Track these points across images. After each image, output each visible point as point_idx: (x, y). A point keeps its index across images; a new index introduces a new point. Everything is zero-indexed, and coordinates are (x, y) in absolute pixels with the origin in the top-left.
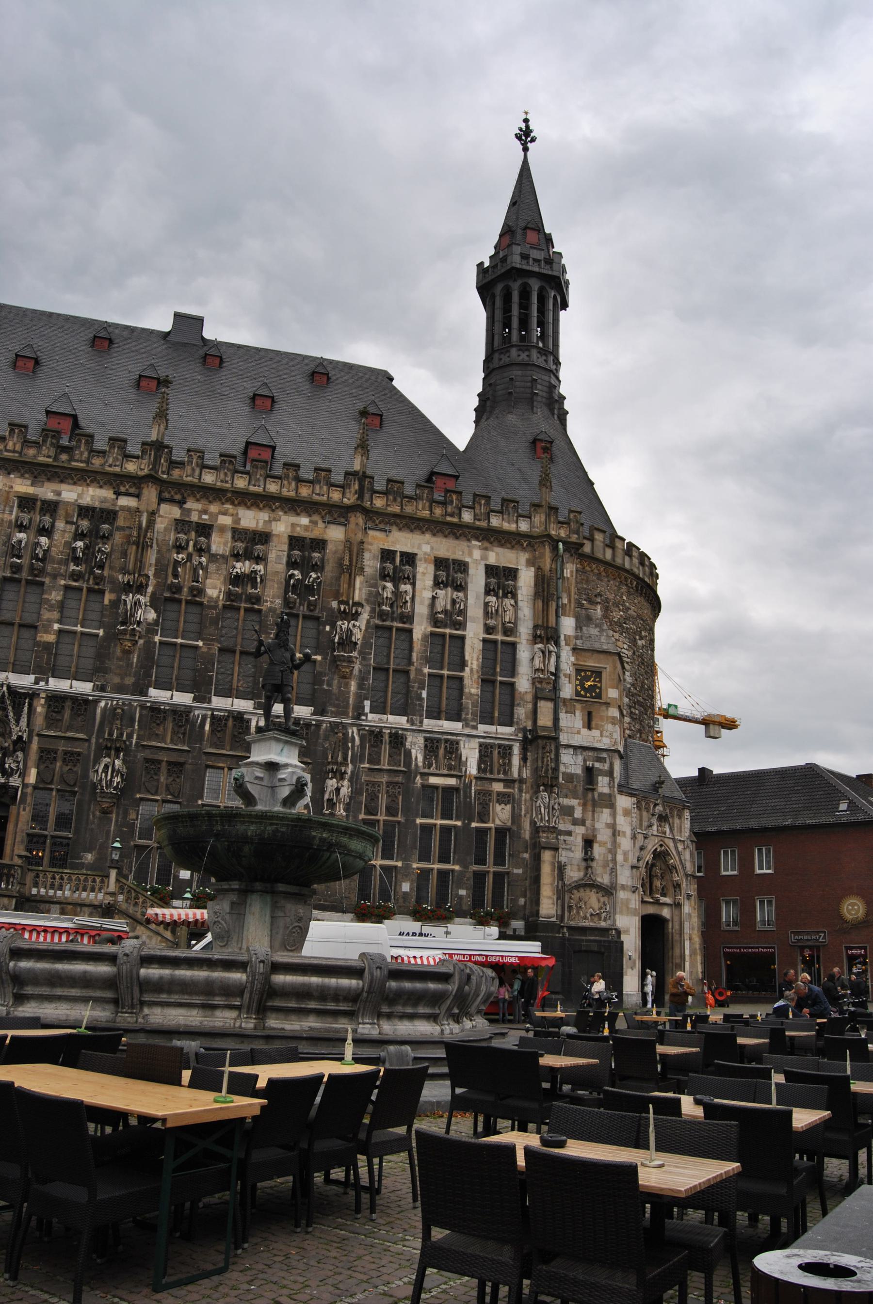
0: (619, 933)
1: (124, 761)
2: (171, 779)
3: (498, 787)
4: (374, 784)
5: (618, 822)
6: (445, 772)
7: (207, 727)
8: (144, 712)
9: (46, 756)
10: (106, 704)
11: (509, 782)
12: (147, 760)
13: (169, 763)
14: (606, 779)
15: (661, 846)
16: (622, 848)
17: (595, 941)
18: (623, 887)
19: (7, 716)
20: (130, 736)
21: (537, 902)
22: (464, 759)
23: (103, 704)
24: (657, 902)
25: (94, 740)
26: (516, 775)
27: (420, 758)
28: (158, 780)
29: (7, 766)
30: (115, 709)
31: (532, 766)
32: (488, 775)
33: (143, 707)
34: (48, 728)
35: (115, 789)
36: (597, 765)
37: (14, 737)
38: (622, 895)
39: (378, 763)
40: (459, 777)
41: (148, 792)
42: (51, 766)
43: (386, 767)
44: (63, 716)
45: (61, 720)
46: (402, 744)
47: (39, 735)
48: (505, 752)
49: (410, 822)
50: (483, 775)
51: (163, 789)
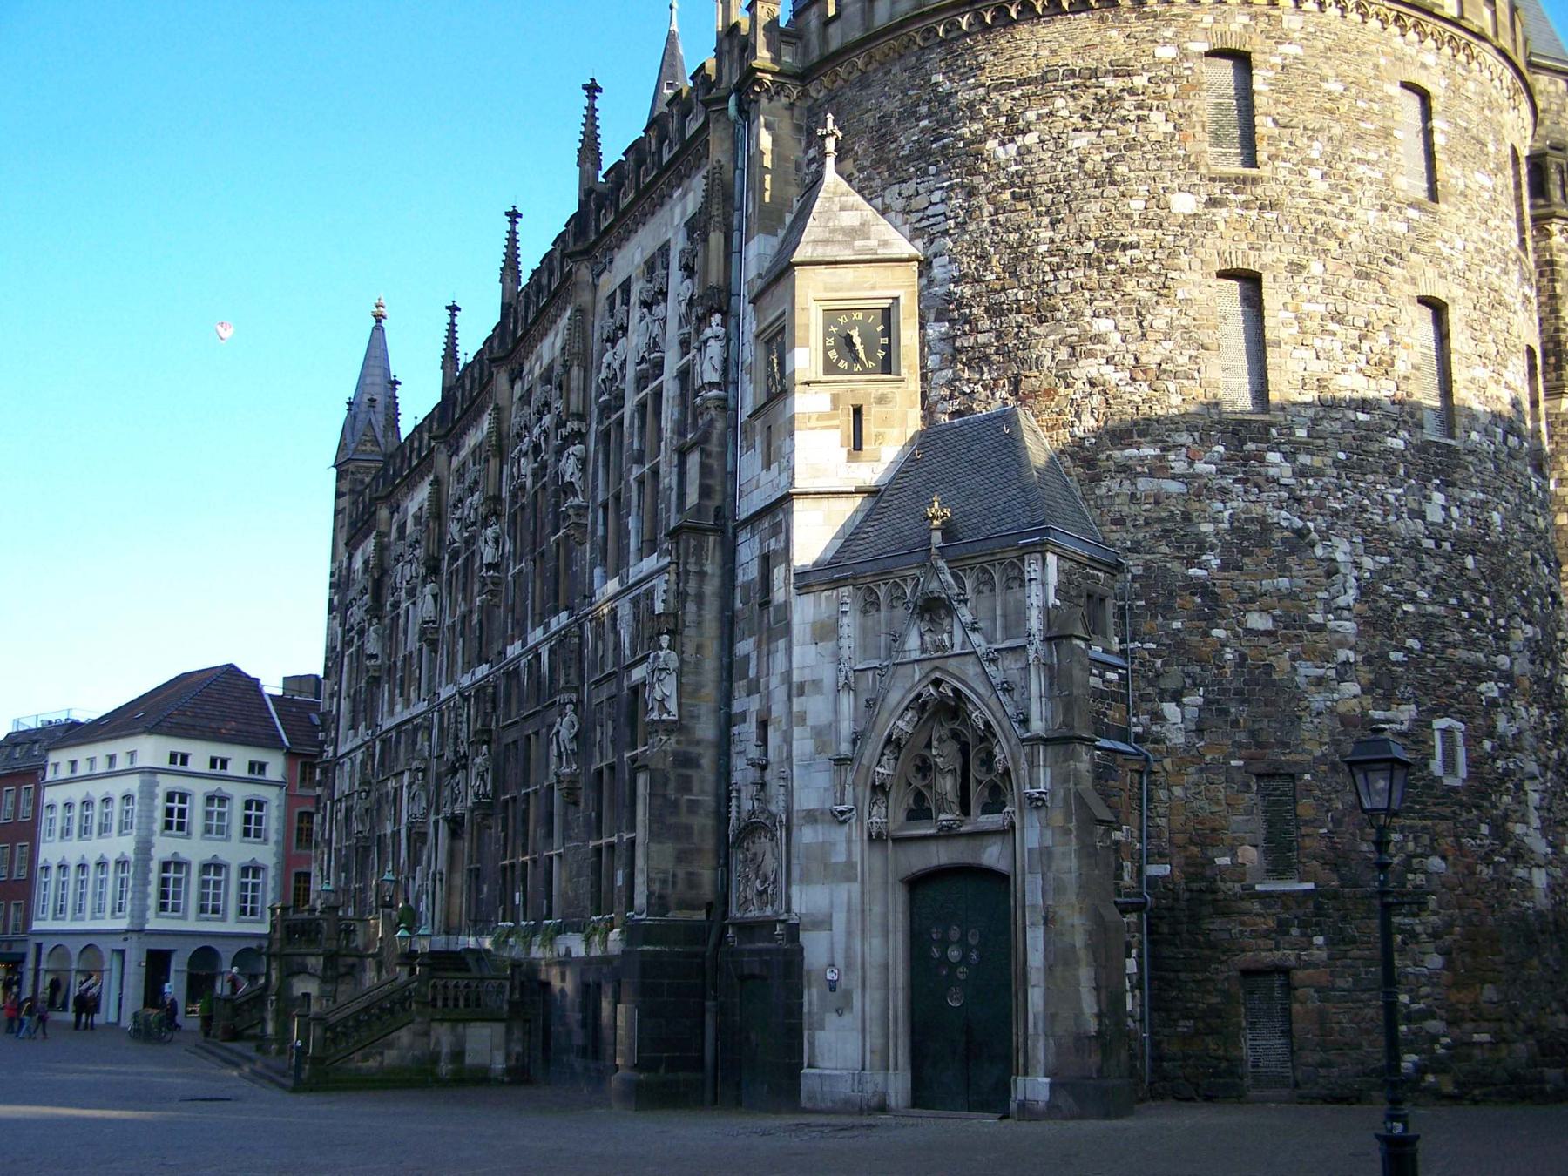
0: (793, 931)
5: (795, 665)
15: (937, 683)
16: (810, 722)
17: (760, 952)
18: (811, 817)
24: (948, 834)
38: (807, 836)
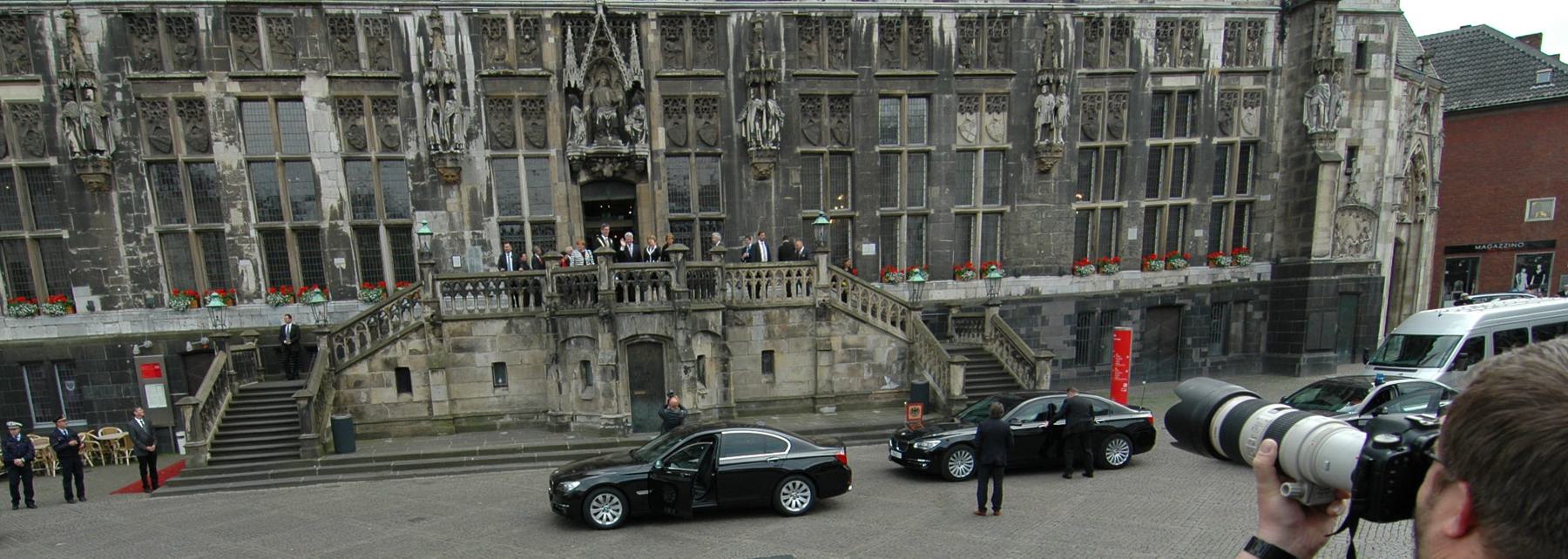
1: (779, 103)
2: (835, 120)
3: (1247, 83)
4: (1092, 96)
6: (1182, 68)
7: (876, 38)
8: (791, 25)
9: (673, 106)
10: (739, 19)
11: (1260, 74)
12: (803, 97)
13: (832, 98)
14: (1382, 57)
19: (611, 54)
20: (777, 63)
21: (1307, 234)
22: (1206, 47)
23: (733, 20)
25: (731, 77)
26: (1269, 65)
27: (1151, 52)
28: (820, 125)
29: (628, 128)
30: (753, 25)
31: (1290, 48)
32: (1235, 68)
33: (788, 17)
34: (667, 65)
35: (775, 143)
36: (1372, 37)
37: (629, 85)
39: (1097, 66)
40: (1199, 73)
41: (809, 141)
42: (682, 121)
43: (1108, 70)
44: (684, 45)
45: (683, 52)
46: (1128, 33)
47: (658, 77)
48: (1257, 29)
49: (1138, 144)
50: (1228, 68)
51: (827, 136)
